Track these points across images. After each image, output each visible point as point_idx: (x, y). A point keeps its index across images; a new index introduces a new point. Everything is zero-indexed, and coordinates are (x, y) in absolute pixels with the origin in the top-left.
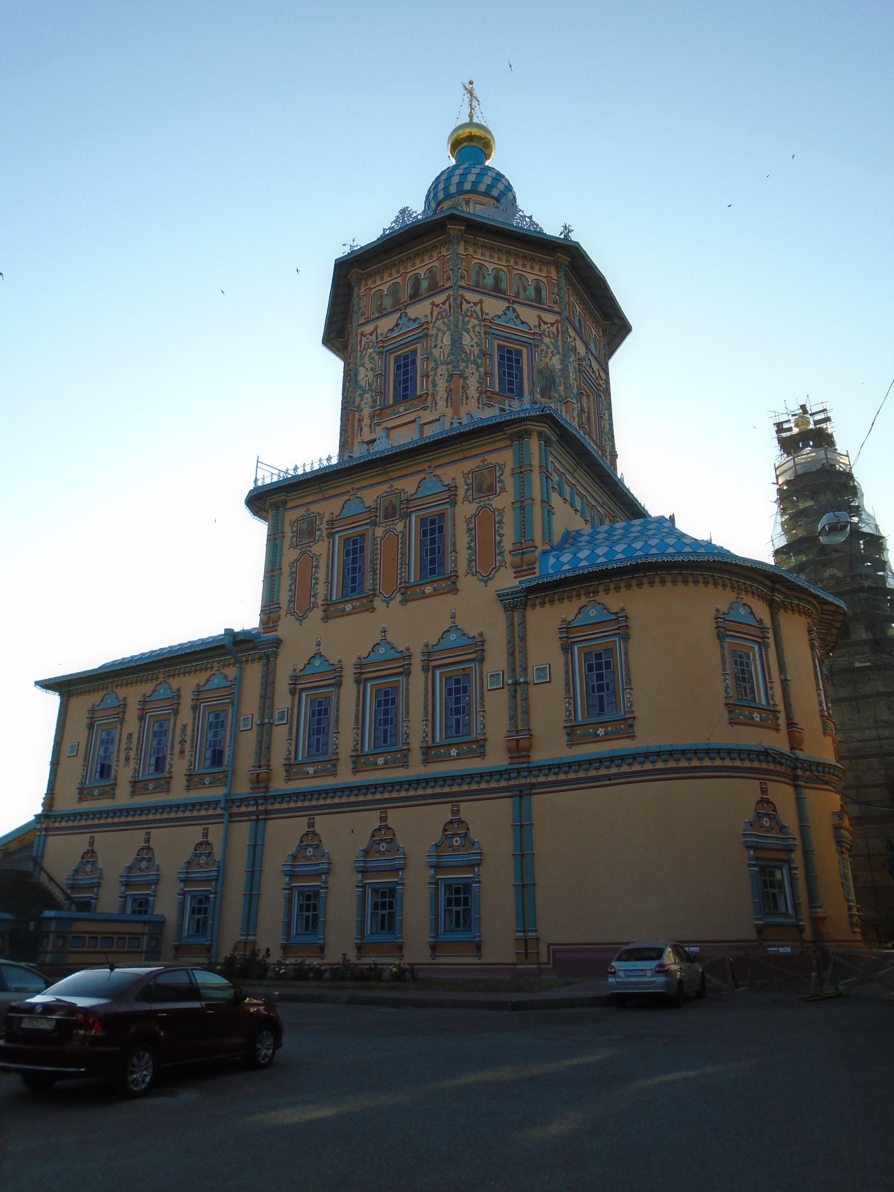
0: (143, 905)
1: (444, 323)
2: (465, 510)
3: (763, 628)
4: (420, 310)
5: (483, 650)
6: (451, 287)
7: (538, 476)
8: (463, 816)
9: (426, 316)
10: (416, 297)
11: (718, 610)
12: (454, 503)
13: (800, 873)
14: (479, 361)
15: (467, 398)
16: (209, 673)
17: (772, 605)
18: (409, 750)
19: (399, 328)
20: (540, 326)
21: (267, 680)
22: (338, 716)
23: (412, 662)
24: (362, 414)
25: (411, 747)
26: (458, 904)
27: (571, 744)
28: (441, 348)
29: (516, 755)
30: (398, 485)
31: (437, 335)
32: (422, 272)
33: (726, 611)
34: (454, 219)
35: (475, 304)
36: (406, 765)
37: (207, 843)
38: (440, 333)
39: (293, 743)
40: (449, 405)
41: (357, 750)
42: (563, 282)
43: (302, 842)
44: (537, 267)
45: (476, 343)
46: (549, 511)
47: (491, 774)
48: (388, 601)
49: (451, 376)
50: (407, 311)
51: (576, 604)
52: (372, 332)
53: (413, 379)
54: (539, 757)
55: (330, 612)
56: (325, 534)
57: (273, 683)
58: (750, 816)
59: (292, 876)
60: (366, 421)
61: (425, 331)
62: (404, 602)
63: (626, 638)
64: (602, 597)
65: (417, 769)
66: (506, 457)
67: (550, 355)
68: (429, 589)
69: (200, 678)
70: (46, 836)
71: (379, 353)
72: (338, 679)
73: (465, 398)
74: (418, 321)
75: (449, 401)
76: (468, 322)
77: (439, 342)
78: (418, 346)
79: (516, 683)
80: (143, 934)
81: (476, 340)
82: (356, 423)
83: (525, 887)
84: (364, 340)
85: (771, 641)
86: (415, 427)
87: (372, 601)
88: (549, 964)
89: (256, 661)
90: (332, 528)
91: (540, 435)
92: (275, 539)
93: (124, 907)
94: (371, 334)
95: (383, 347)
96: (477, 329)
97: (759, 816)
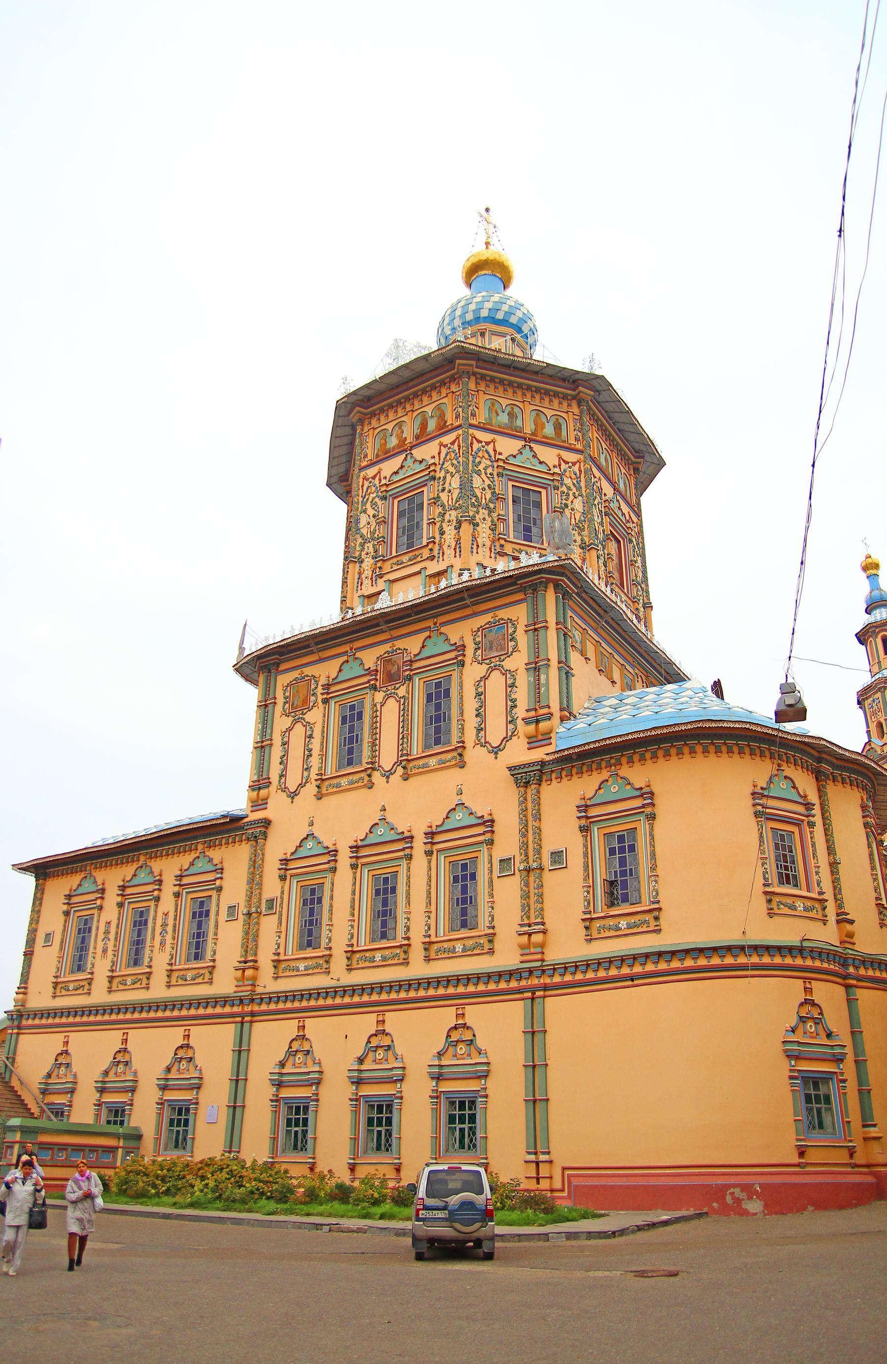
0: (118, 1113)
1: (453, 465)
2: (473, 671)
3: (809, 806)
4: (427, 452)
5: (493, 832)
6: (460, 426)
7: (555, 631)
8: (469, 1021)
9: (434, 457)
10: (422, 438)
11: (755, 786)
12: (462, 664)
13: (852, 1086)
14: (492, 506)
15: (478, 546)
16: (193, 855)
17: (818, 776)
18: (409, 945)
19: (404, 470)
20: (560, 465)
21: (255, 862)
22: (331, 906)
23: (414, 844)
24: (363, 565)
25: (412, 942)
26: (462, 1120)
27: (589, 941)
28: (450, 491)
29: (527, 951)
30: (400, 644)
31: (445, 478)
32: (429, 410)
33: (765, 786)
34: (463, 353)
35: (487, 443)
36: (406, 963)
37: (188, 1046)
38: (448, 476)
39: (283, 935)
41: (352, 945)
42: (586, 418)
43: (290, 1047)
44: (556, 402)
45: (489, 486)
46: (567, 673)
47: (500, 975)
48: (388, 775)
49: (459, 523)
51: (595, 779)
52: (375, 476)
53: (419, 525)
54: (556, 954)
55: (324, 787)
56: (320, 697)
57: (262, 866)
58: (794, 1021)
59: (279, 1085)
60: (368, 573)
62: (406, 778)
63: (652, 817)
64: (624, 771)
65: (418, 969)
66: (520, 613)
67: (571, 497)
68: (432, 761)
69: (185, 860)
70: (18, 1034)
71: (384, 498)
72: (332, 864)
73: (475, 547)
74: (424, 463)
75: (458, 550)
76: (480, 463)
77: (447, 486)
78: (425, 489)
79: (528, 870)
80: (117, 1148)
81: (487, 482)
82: (357, 576)
83: (536, 1103)
84: (366, 484)
85: (818, 820)
86: (418, 580)
87: (369, 776)
88: (562, 1190)
89: (244, 843)
90: (328, 693)
91: (557, 587)
92: (266, 706)
93: (98, 1115)
94: (374, 478)
96: (489, 470)
97: (802, 1020)
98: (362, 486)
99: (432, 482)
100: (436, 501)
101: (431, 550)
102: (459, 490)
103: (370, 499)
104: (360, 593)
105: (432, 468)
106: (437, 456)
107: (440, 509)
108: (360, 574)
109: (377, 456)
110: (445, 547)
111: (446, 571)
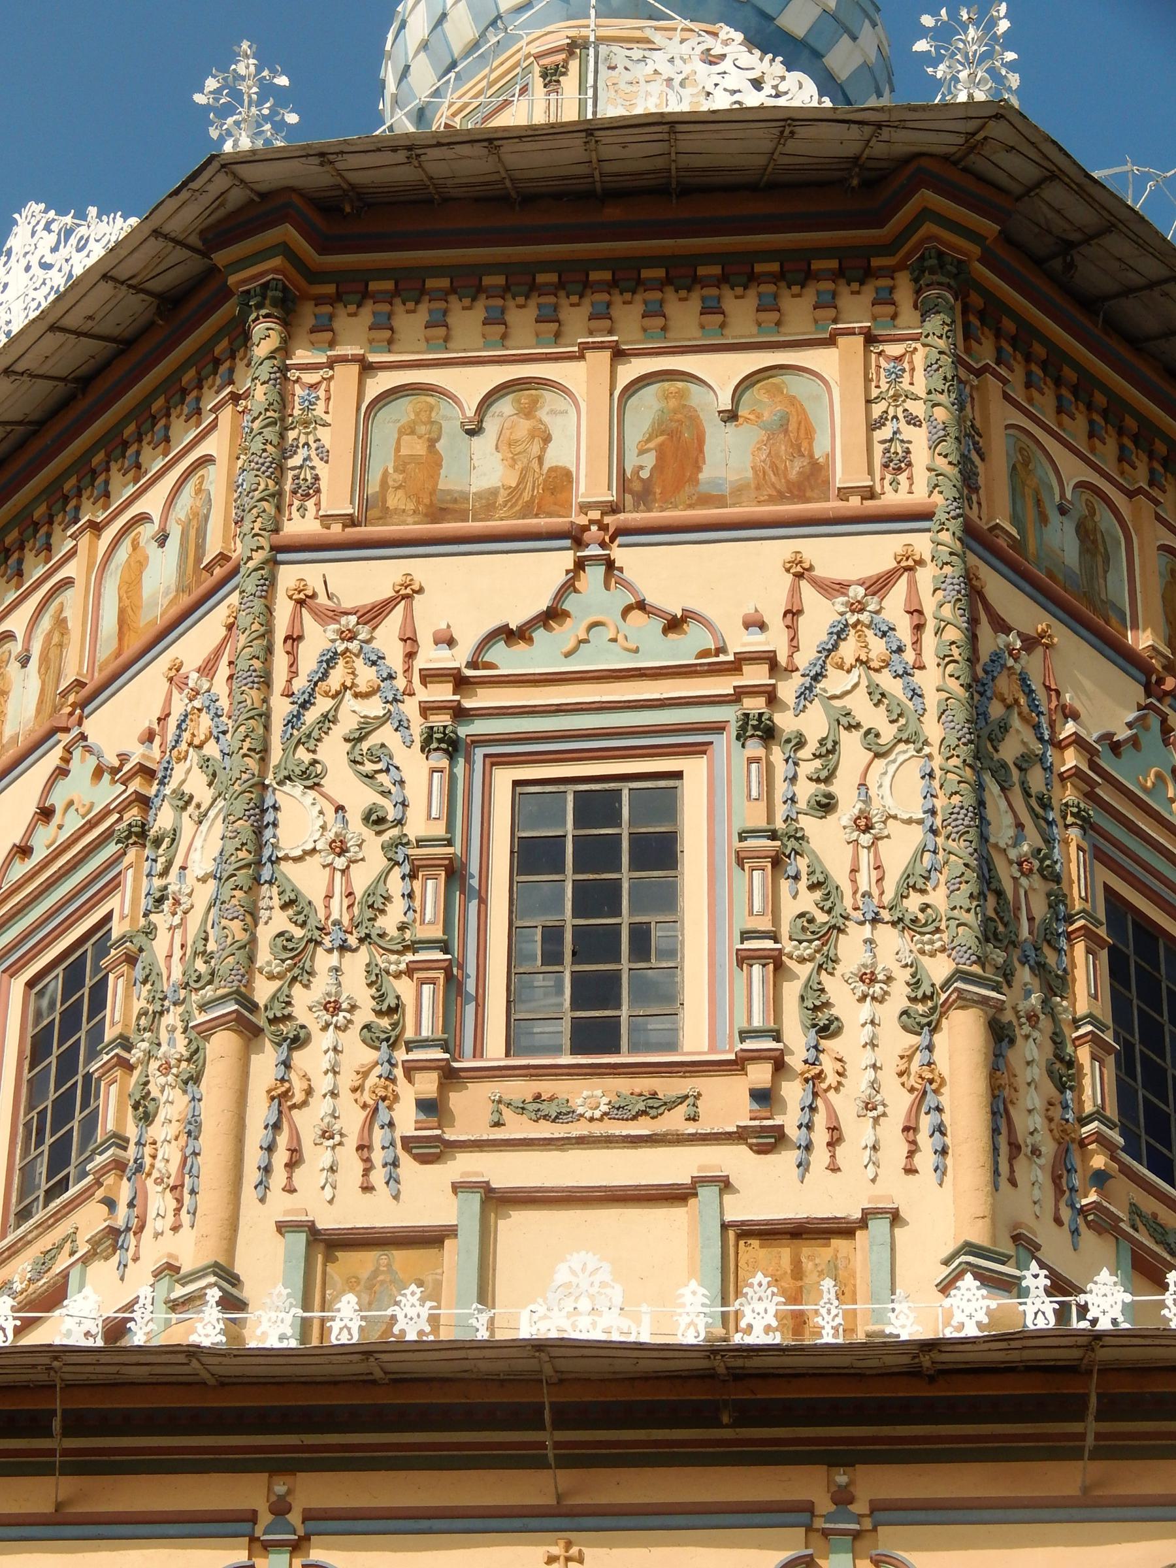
1: (879, 697)
6: (918, 517)
10: (663, 498)
19: (566, 633)
24: (311, 1061)
28: (864, 824)
31: (829, 750)
40: (926, 1159)
50: (619, 555)
61: (754, 705)
76: (1004, 728)
77: (844, 788)
78: (694, 770)
82: (259, 1112)
94: (374, 614)
95: (460, 714)
96: (1037, 780)
98: (294, 639)
99: (755, 748)
100: (779, 851)
101: (763, 1097)
102: (917, 835)
103: (347, 723)
104: (280, 1206)
105: (756, 675)
106: (776, 622)
107: (808, 901)
108: (281, 1098)
109: (369, 506)
110: (846, 1104)
111: (844, 1229)
